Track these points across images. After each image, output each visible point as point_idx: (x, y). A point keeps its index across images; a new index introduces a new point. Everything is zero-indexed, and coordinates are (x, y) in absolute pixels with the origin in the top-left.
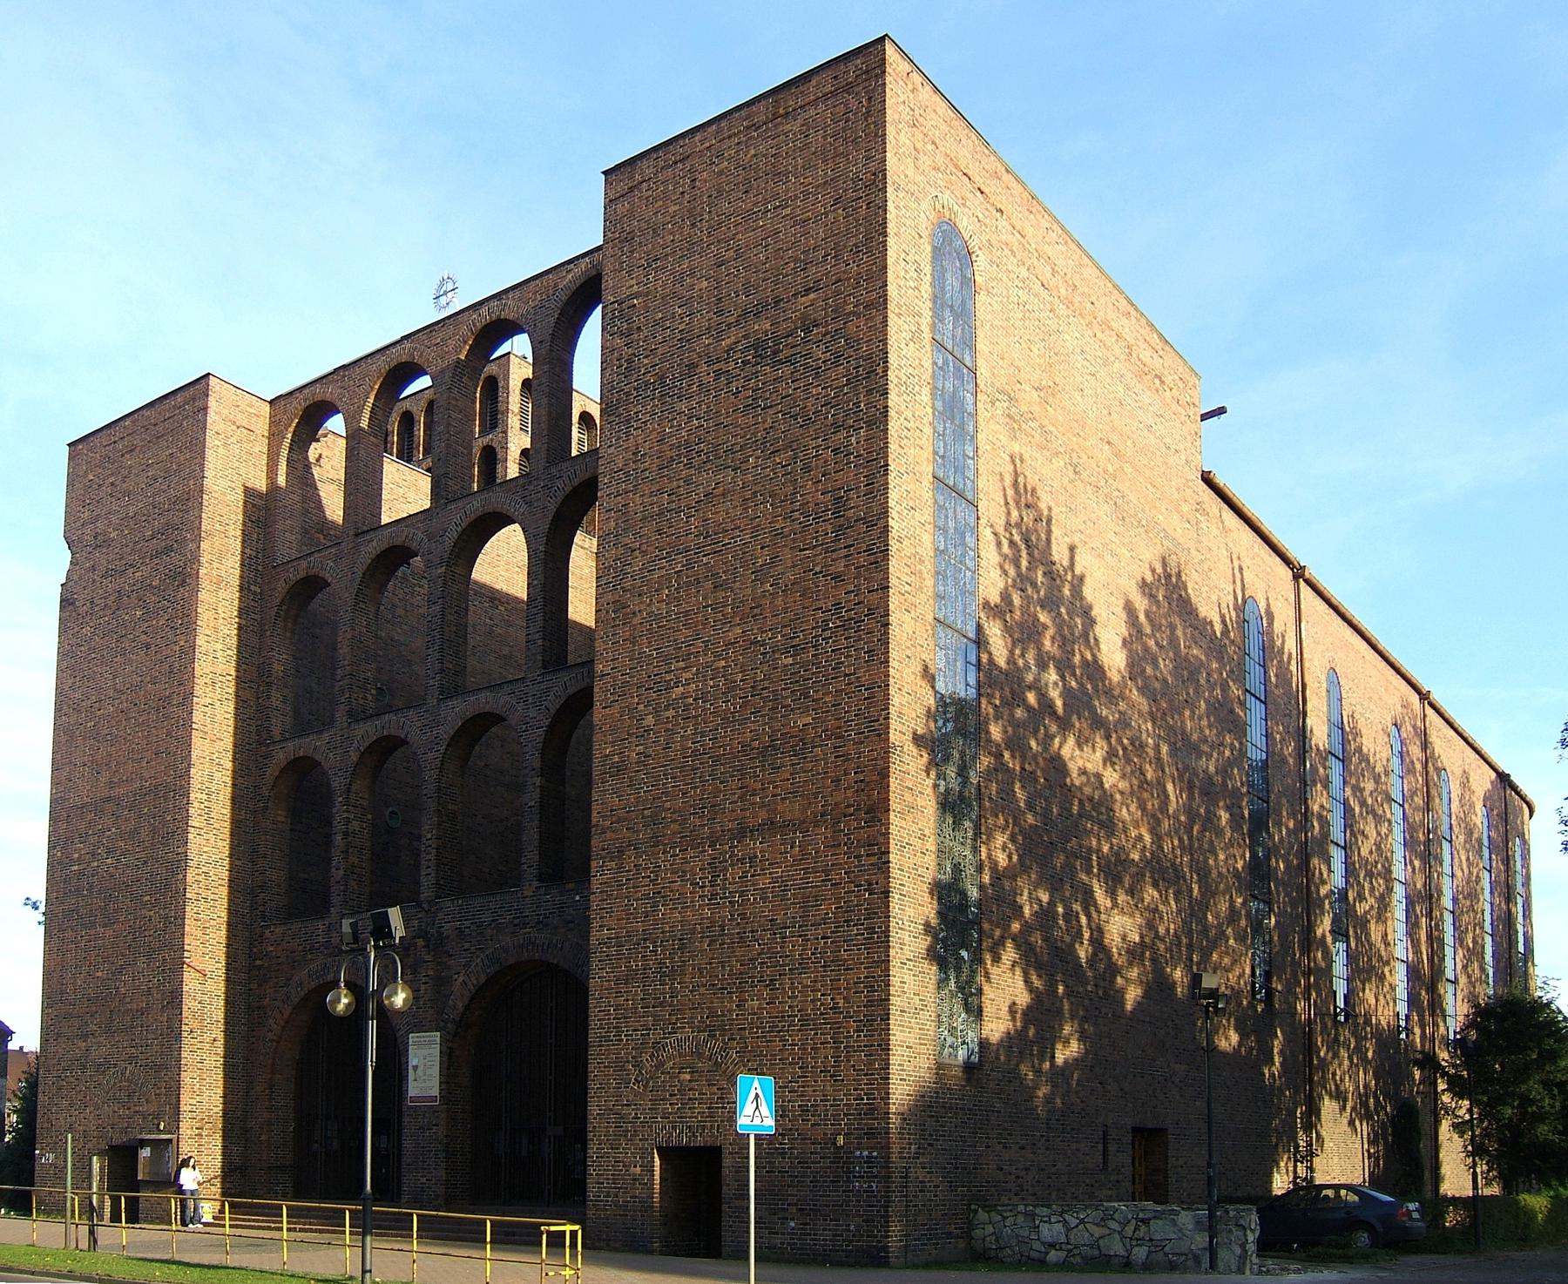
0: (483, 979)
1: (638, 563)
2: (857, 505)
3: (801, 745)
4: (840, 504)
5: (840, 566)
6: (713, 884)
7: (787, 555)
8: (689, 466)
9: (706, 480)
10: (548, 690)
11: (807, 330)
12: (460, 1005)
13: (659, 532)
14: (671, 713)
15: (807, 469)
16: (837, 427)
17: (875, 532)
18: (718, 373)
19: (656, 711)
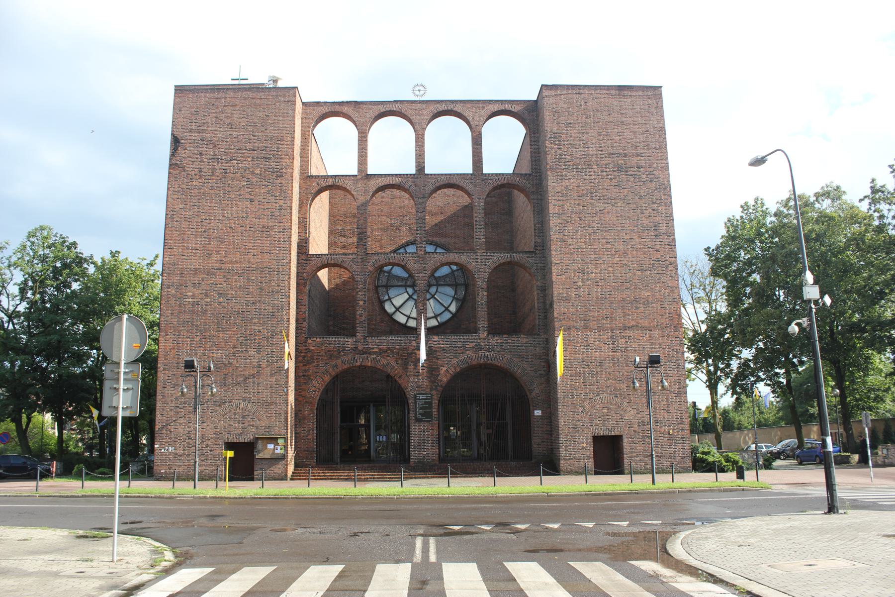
0: (458, 370)
1: (570, 227)
2: (663, 228)
3: (647, 303)
4: (656, 227)
5: (658, 247)
6: (613, 344)
7: (637, 239)
8: (592, 198)
9: (600, 206)
10: (489, 259)
11: (639, 168)
12: (445, 380)
13: (580, 218)
14: (590, 282)
15: (642, 213)
16: (654, 203)
17: (671, 239)
18: (602, 171)
19: (583, 281)
